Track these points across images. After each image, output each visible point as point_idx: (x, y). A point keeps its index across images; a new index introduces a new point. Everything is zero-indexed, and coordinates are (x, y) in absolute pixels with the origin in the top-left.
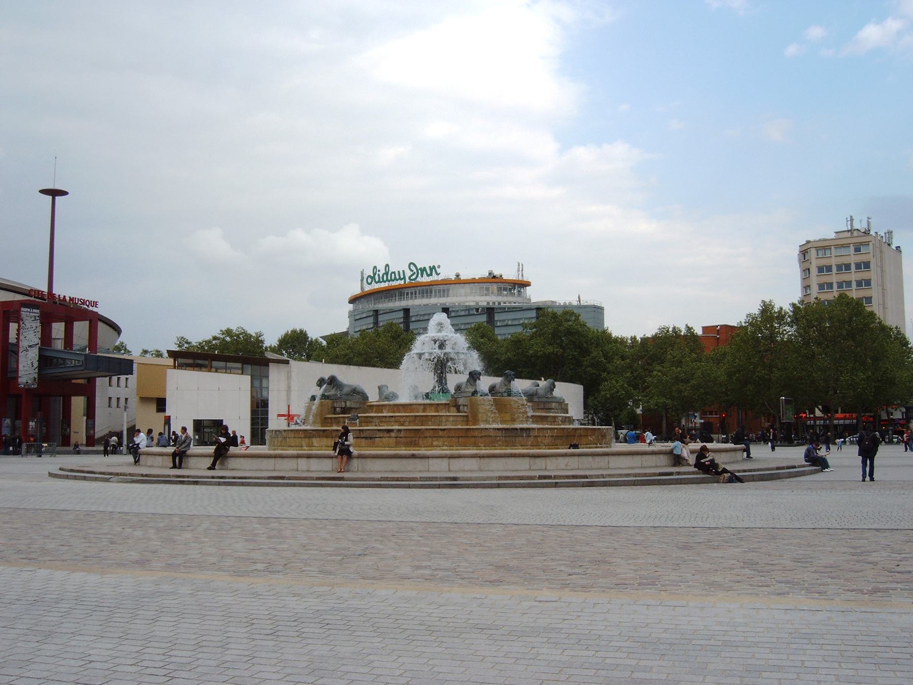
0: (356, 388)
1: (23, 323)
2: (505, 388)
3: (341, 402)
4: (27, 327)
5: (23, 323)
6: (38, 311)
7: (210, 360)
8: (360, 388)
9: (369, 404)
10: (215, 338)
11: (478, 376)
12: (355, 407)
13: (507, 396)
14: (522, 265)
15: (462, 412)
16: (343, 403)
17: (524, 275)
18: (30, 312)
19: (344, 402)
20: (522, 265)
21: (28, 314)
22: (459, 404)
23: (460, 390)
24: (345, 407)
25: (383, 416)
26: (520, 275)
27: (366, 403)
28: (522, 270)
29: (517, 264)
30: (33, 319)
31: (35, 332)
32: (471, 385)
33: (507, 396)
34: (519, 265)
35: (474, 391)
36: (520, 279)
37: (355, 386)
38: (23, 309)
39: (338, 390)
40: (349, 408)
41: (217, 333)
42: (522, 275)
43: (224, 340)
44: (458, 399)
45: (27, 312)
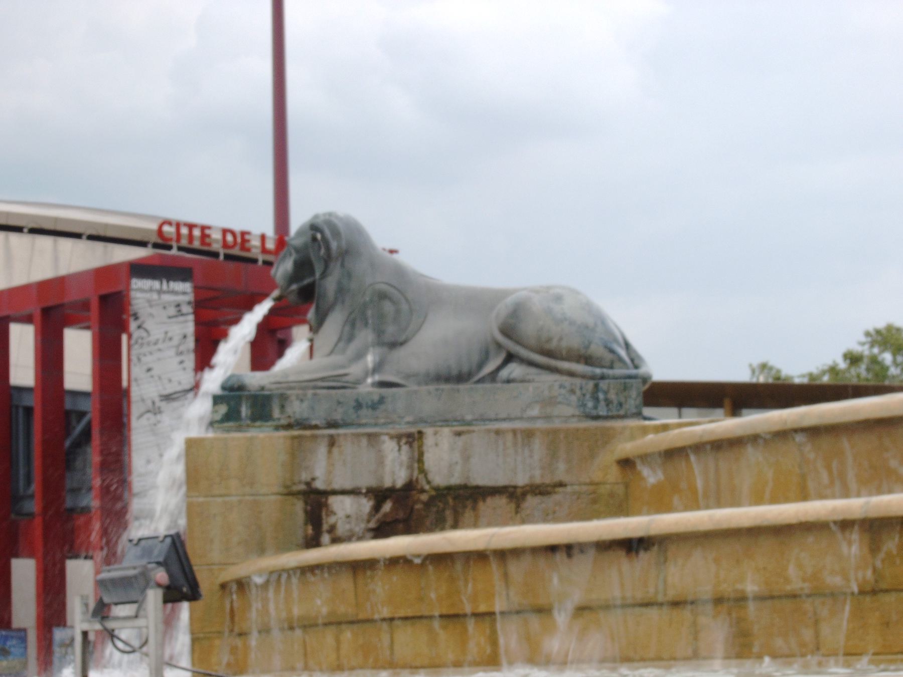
0: (518, 311)
1: (139, 327)
3: (372, 438)
4: (152, 338)
5: (139, 327)
6: (187, 287)
7: (727, 402)
8: (568, 308)
9: (626, 448)
10: (853, 359)
12: (500, 479)
16: (389, 446)
18: (160, 292)
19: (398, 437)
21: (155, 296)
24: (410, 486)
25: (552, 549)
27: (607, 437)
30: (172, 311)
31: (181, 353)
37: (510, 300)
38: (137, 283)
39: (365, 336)
40: (445, 494)
41: (855, 342)
43: (874, 360)
45: (151, 290)
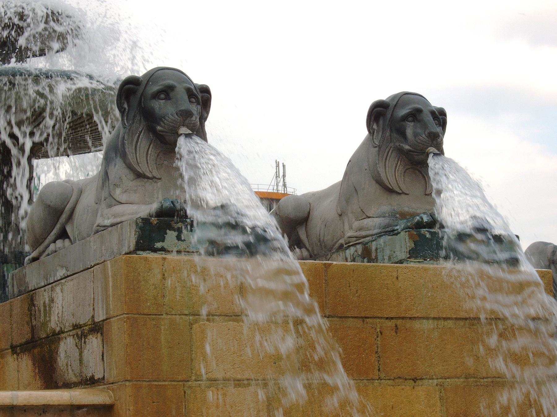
2: (385, 209)
11: (195, 109)
13: (414, 254)
14: (284, 166)
15: (67, 386)
17: (288, 185)
20: (284, 166)
22: (54, 324)
23: (63, 235)
26: (281, 184)
28: (284, 176)
29: (274, 165)
32: (139, 176)
33: (414, 254)
34: (278, 166)
35: (162, 213)
36: (281, 190)
42: (285, 185)
44: (43, 297)
